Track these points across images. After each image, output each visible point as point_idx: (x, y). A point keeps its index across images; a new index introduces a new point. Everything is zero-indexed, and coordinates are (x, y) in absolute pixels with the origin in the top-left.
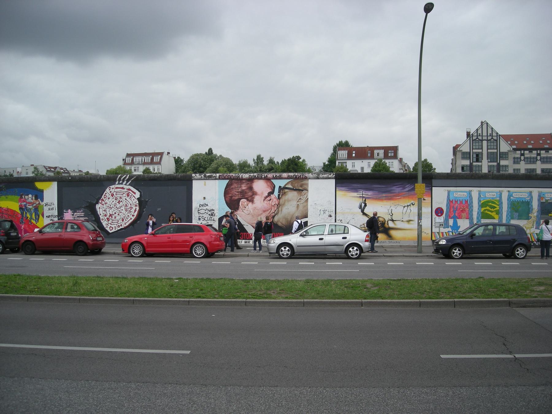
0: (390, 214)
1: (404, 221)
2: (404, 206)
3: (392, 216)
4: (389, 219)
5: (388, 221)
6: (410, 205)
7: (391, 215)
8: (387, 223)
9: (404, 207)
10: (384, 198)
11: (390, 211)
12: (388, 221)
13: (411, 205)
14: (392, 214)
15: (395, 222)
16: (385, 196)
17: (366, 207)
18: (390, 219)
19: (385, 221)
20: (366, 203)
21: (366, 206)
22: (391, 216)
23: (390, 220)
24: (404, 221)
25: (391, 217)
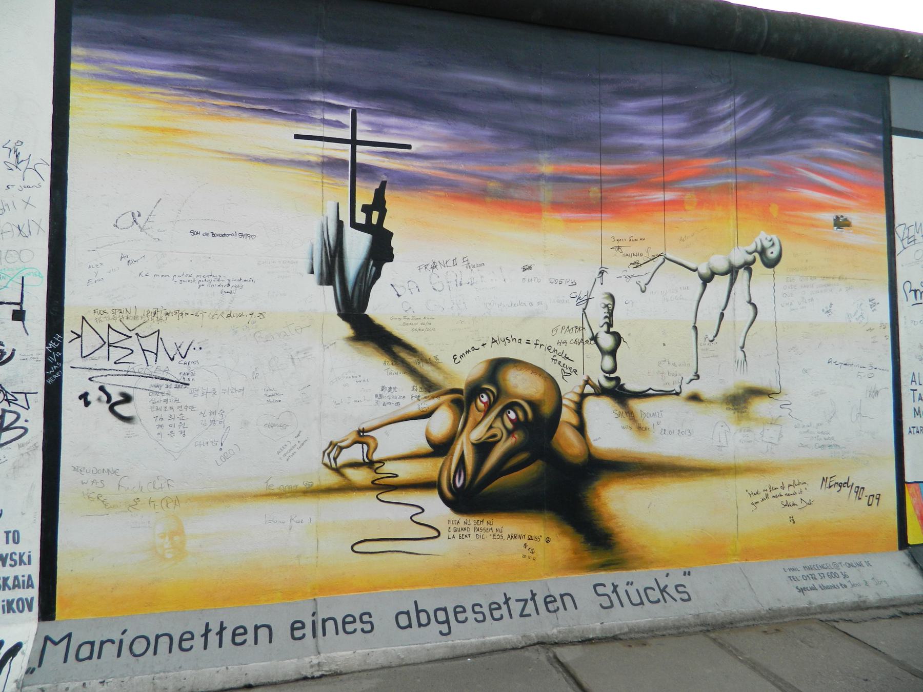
0: (594, 338)
3: (613, 353)
7: (607, 341)
10: (546, 193)
11: (597, 315)
14: (618, 338)
15: (636, 405)
16: (557, 179)
18: (599, 378)
22: (603, 352)
23: (601, 392)
25: (608, 363)
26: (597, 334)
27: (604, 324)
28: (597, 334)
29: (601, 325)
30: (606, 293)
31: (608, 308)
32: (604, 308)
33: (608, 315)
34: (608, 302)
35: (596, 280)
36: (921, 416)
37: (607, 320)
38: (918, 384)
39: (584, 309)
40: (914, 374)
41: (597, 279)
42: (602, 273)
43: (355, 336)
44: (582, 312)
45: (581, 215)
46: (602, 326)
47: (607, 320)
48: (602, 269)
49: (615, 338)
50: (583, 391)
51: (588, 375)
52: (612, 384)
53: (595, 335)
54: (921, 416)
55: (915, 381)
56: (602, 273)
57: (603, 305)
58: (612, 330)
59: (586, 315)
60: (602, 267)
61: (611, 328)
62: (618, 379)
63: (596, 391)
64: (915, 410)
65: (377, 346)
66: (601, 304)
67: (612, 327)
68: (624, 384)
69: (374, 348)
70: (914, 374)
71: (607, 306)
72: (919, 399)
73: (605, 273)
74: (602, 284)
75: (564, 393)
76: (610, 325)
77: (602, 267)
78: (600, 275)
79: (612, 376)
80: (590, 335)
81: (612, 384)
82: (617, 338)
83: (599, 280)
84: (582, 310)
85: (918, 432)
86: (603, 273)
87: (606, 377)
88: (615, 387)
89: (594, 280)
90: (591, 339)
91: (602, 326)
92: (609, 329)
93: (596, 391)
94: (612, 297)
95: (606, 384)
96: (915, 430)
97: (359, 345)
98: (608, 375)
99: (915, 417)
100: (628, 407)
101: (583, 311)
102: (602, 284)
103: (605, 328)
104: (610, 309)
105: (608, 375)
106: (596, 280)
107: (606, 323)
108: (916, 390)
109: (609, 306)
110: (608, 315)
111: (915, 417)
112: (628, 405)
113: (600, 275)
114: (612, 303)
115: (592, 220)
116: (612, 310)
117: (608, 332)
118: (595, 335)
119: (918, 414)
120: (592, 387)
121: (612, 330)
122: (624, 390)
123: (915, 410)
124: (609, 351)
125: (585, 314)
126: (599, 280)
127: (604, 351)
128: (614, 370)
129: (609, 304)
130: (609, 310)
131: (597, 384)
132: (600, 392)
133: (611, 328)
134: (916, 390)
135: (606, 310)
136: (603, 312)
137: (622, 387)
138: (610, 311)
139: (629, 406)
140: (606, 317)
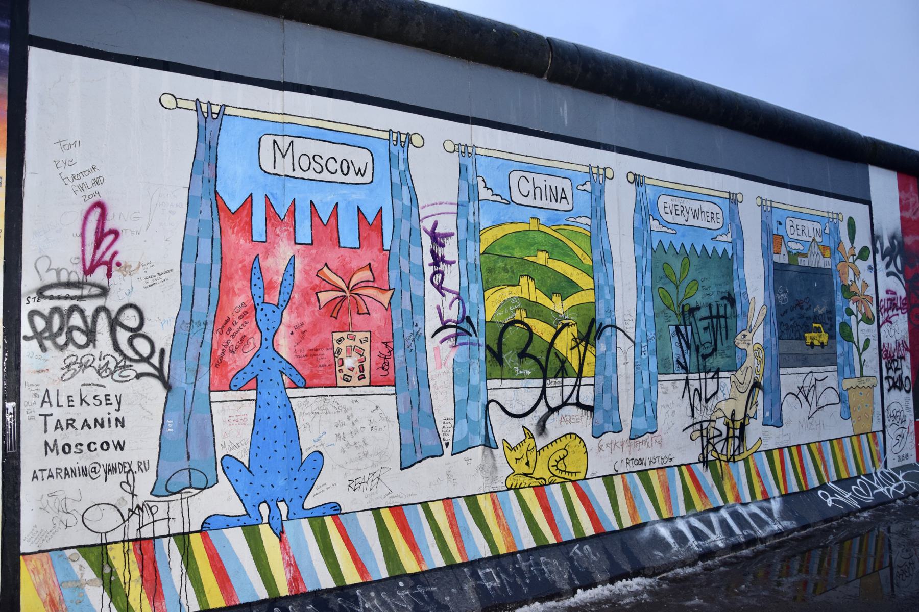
36: (58, 453)
38: (54, 403)
40: (47, 391)
54: (58, 453)
55: (50, 402)
64: (46, 443)
70: (47, 391)
72: (56, 428)
85: (51, 476)
96: (46, 474)
99: (46, 454)
108: (51, 415)
111: (46, 454)
119: (52, 451)
123: (46, 443)
134: (51, 415)
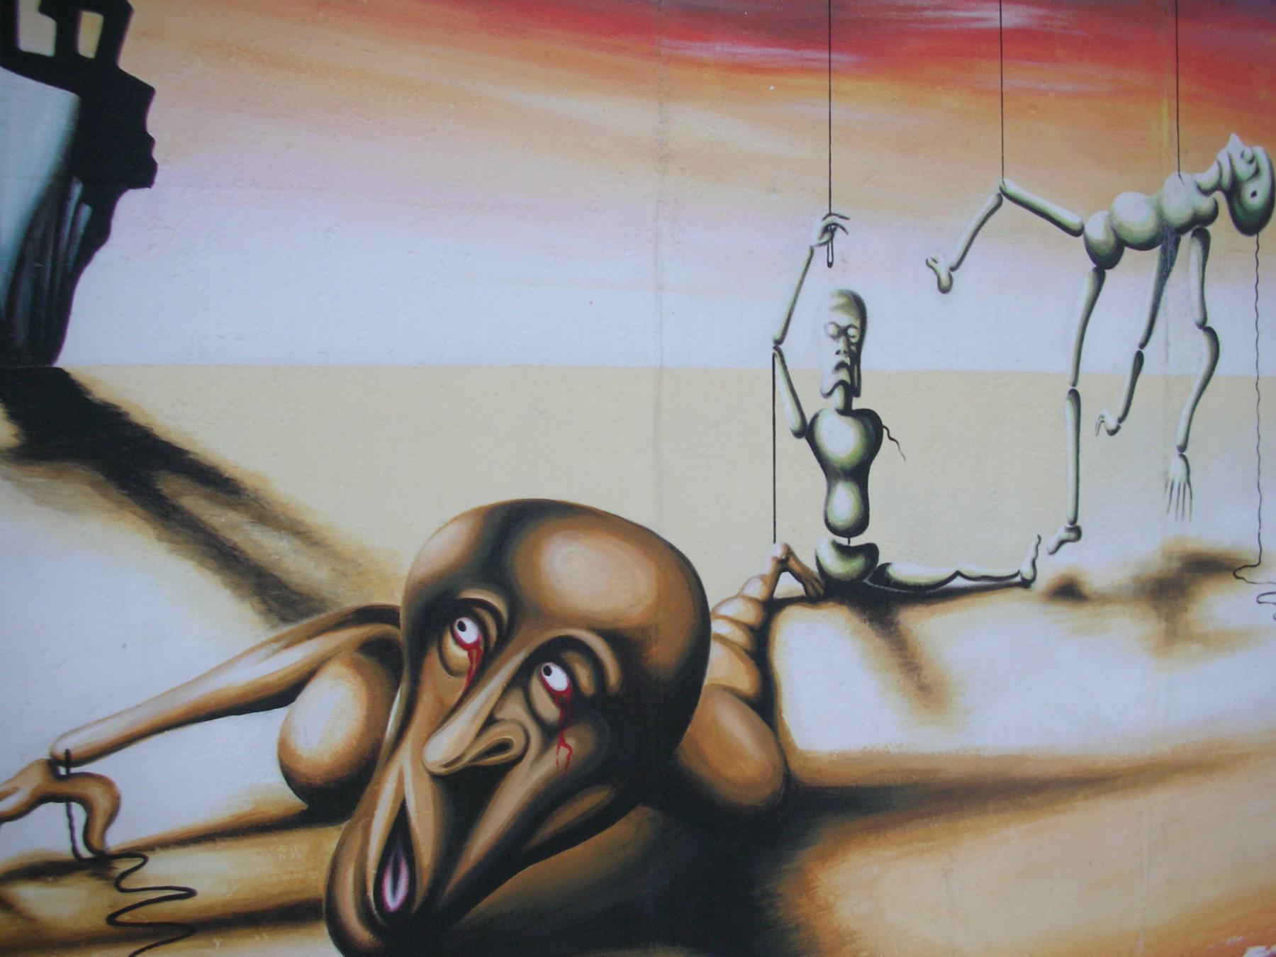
0: (807, 431)
1: (1104, 599)
2: (1098, 232)
3: (858, 474)
4: (784, 564)
5: (772, 607)
6: (1199, 225)
8: (745, 681)
9: (1104, 261)
12: (772, 607)
13: (1222, 229)
14: (872, 427)
17: (131, 205)
19: (703, 615)
20: (130, 61)
21: (143, 174)
22: (832, 472)
24: (1104, 599)
25: (844, 503)
26: (815, 417)
27: (836, 385)
28: (815, 417)
29: (828, 390)
30: (843, 294)
31: (848, 337)
32: (835, 337)
33: (848, 361)
34: (845, 319)
35: (812, 252)
37: (844, 375)
39: (778, 342)
41: (817, 250)
42: (830, 230)
43: (22, 447)
44: (772, 351)
45: (772, 51)
46: (830, 394)
47: (844, 375)
48: (830, 220)
49: (865, 427)
50: (772, 592)
51: (788, 542)
52: (857, 564)
53: (809, 420)
56: (830, 230)
57: (833, 330)
58: (857, 404)
59: (783, 361)
60: (830, 214)
61: (855, 400)
62: (870, 551)
63: (810, 588)
65: (101, 477)
66: (826, 327)
67: (858, 394)
68: (888, 564)
69: (92, 484)
71: (843, 332)
73: (839, 233)
74: (830, 265)
75: (717, 601)
76: (852, 389)
77: (830, 214)
78: (826, 237)
79: (856, 541)
80: (795, 423)
81: (857, 564)
82: (870, 427)
83: (821, 253)
84: (772, 345)
86: (833, 232)
87: (839, 548)
88: (864, 574)
89: (808, 253)
90: (798, 434)
91: (830, 394)
92: (848, 402)
93: (810, 588)
94: (857, 305)
95: (837, 566)
97: (38, 477)
98: (843, 541)
100: (897, 630)
101: (775, 348)
102: (830, 265)
103: (838, 398)
104: (853, 340)
105: (843, 541)
106: (812, 252)
107: (841, 383)
109: (851, 332)
110: (848, 361)
112: (898, 623)
113: (826, 237)
114: (857, 324)
115: (802, 70)
116: (859, 345)
117: (846, 411)
118: (809, 420)
120: (798, 577)
121: (857, 404)
122: (889, 581)
124: (848, 467)
125: (781, 355)
126: (821, 253)
127: (835, 469)
128: (861, 524)
129: (849, 326)
130: (849, 344)
131: (814, 569)
132: (822, 592)
133: (855, 400)
135: (841, 345)
136: (832, 352)
137: (879, 573)
138: (853, 348)
139: (901, 627)
140: (840, 366)
